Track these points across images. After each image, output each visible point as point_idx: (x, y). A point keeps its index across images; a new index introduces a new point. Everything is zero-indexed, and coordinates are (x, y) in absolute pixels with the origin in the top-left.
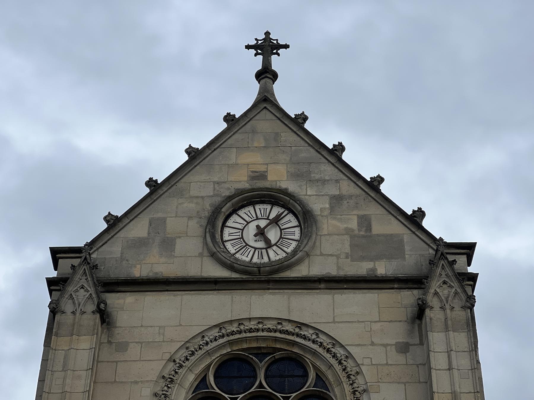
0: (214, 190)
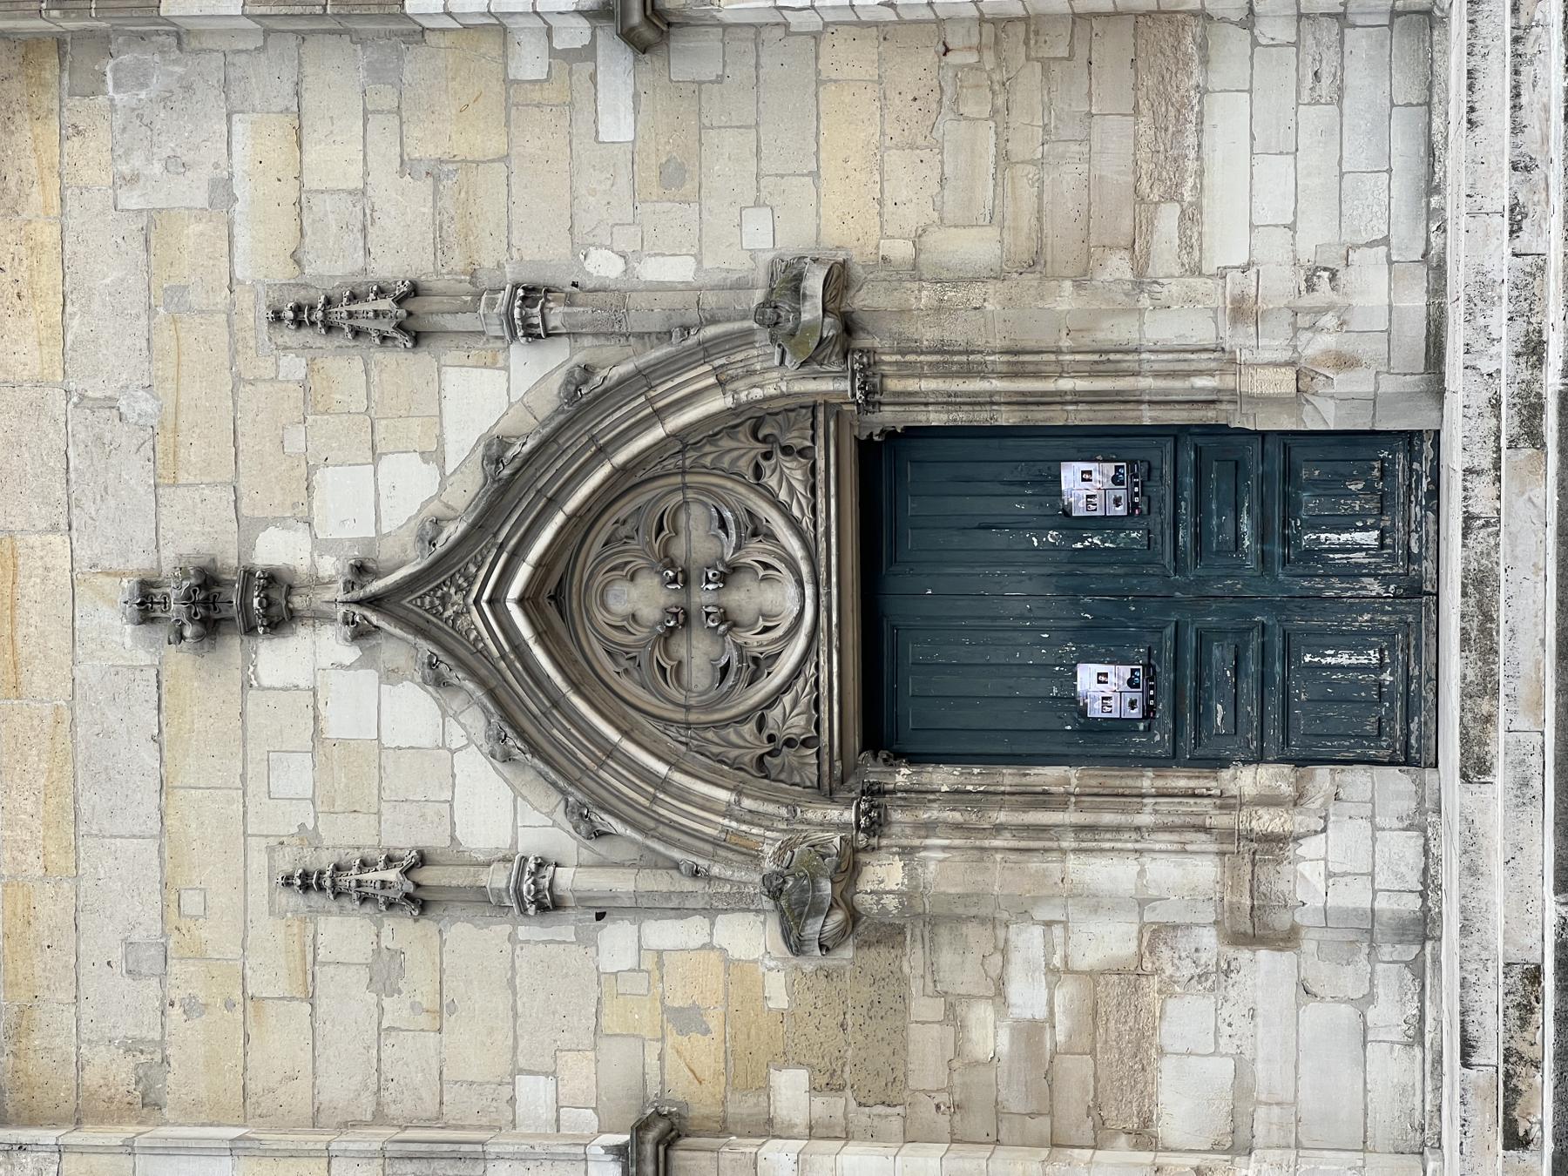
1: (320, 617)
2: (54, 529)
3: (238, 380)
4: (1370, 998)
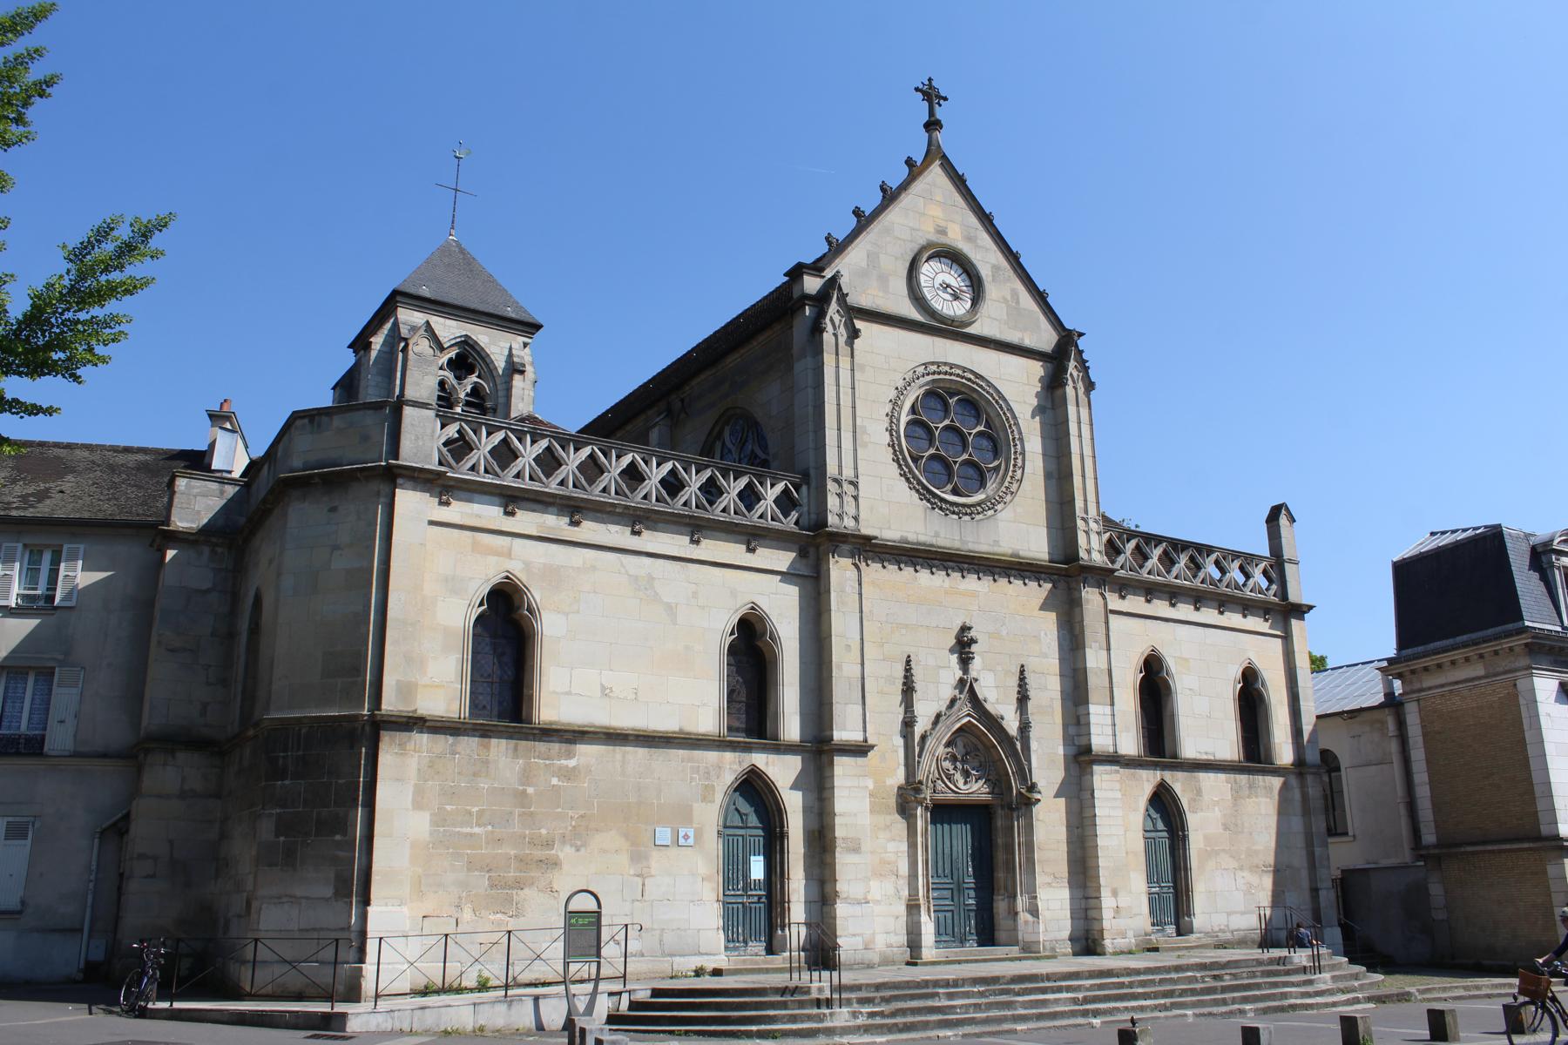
0: (912, 235)
1: (965, 670)
3: (1010, 656)
4: (896, 934)
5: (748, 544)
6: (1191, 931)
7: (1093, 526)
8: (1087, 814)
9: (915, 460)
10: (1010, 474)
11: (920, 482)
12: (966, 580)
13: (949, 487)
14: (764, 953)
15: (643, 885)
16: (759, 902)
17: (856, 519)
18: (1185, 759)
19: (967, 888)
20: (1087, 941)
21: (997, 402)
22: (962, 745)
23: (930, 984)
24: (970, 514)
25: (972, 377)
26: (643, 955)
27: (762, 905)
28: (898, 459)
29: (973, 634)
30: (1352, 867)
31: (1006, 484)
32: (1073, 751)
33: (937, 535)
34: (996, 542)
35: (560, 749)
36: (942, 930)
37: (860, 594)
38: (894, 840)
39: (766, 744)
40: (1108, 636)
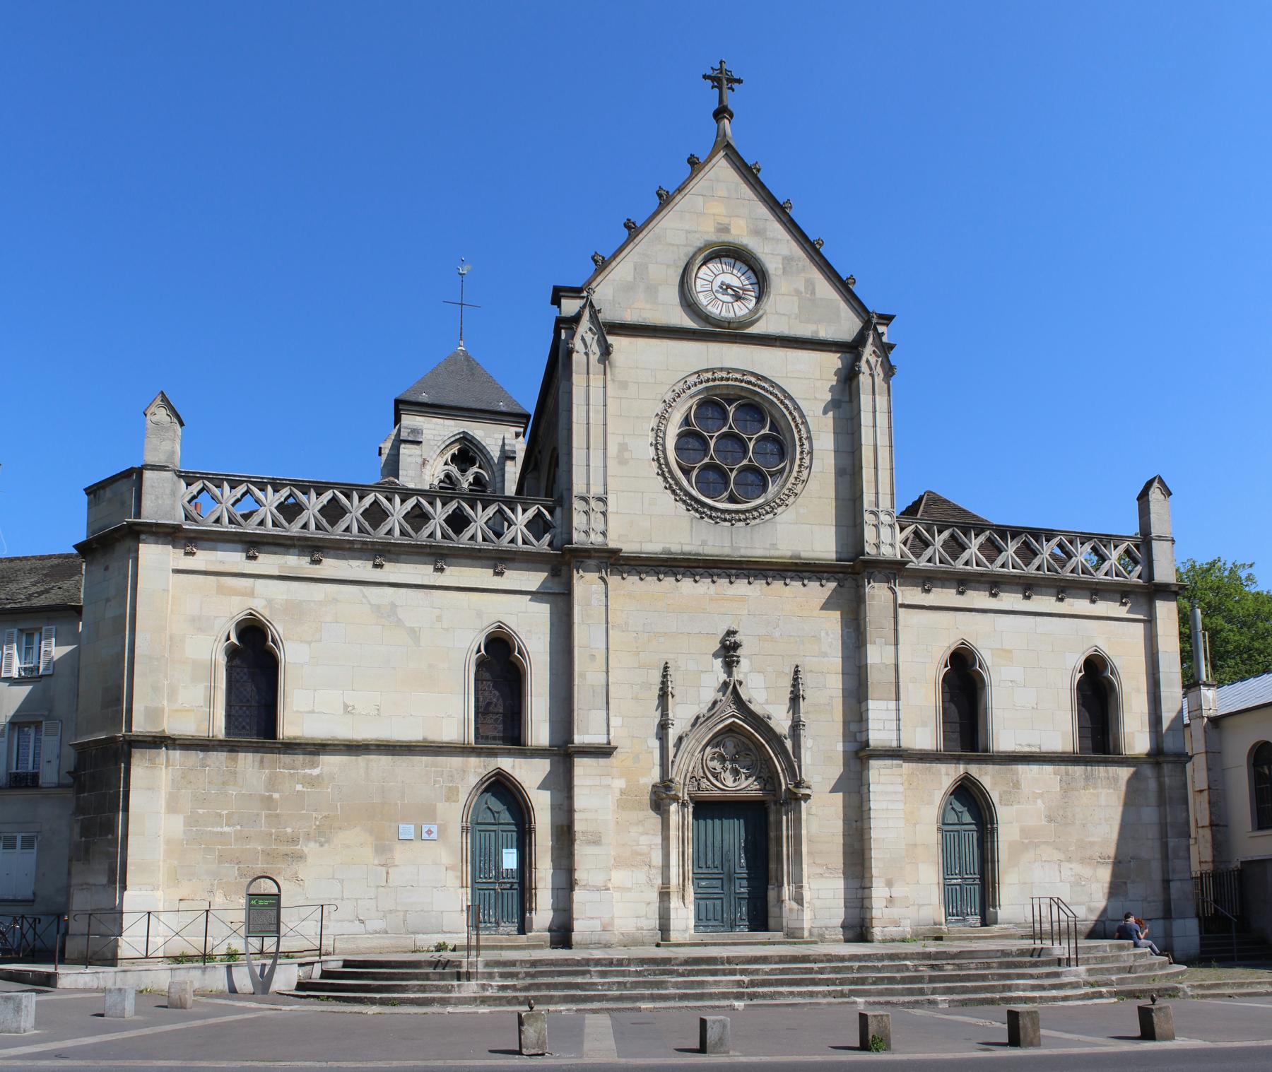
1: (730, 674)
2: (749, 611)
3: (783, 656)
4: (647, 918)
5: (495, 567)
6: (996, 922)
7: (884, 518)
8: (865, 808)
9: (686, 472)
10: (794, 474)
11: (687, 494)
12: (734, 585)
13: (726, 494)
14: (516, 933)
15: (387, 873)
16: (511, 888)
17: (604, 534)
18: (998, 752)
19: (738, 878)
20: (858, 929)
21: (782, 402)
22: (733, 745)
23: (591, 963)
24: (745, 520)
25: (753, 380)
26: (387, 933)
27: (515, 892)
28: (663, 472)
29: (738, 638)
30: (1249, 859)
31: (789, 485)
32: (853, 747)
33: (704, 543)
34: (774, 546)
35: (304, 760)
36: (703, 916)
37: (607, 606)
38: (647, 834)
39: (510, 749)
40: (896, 630)
